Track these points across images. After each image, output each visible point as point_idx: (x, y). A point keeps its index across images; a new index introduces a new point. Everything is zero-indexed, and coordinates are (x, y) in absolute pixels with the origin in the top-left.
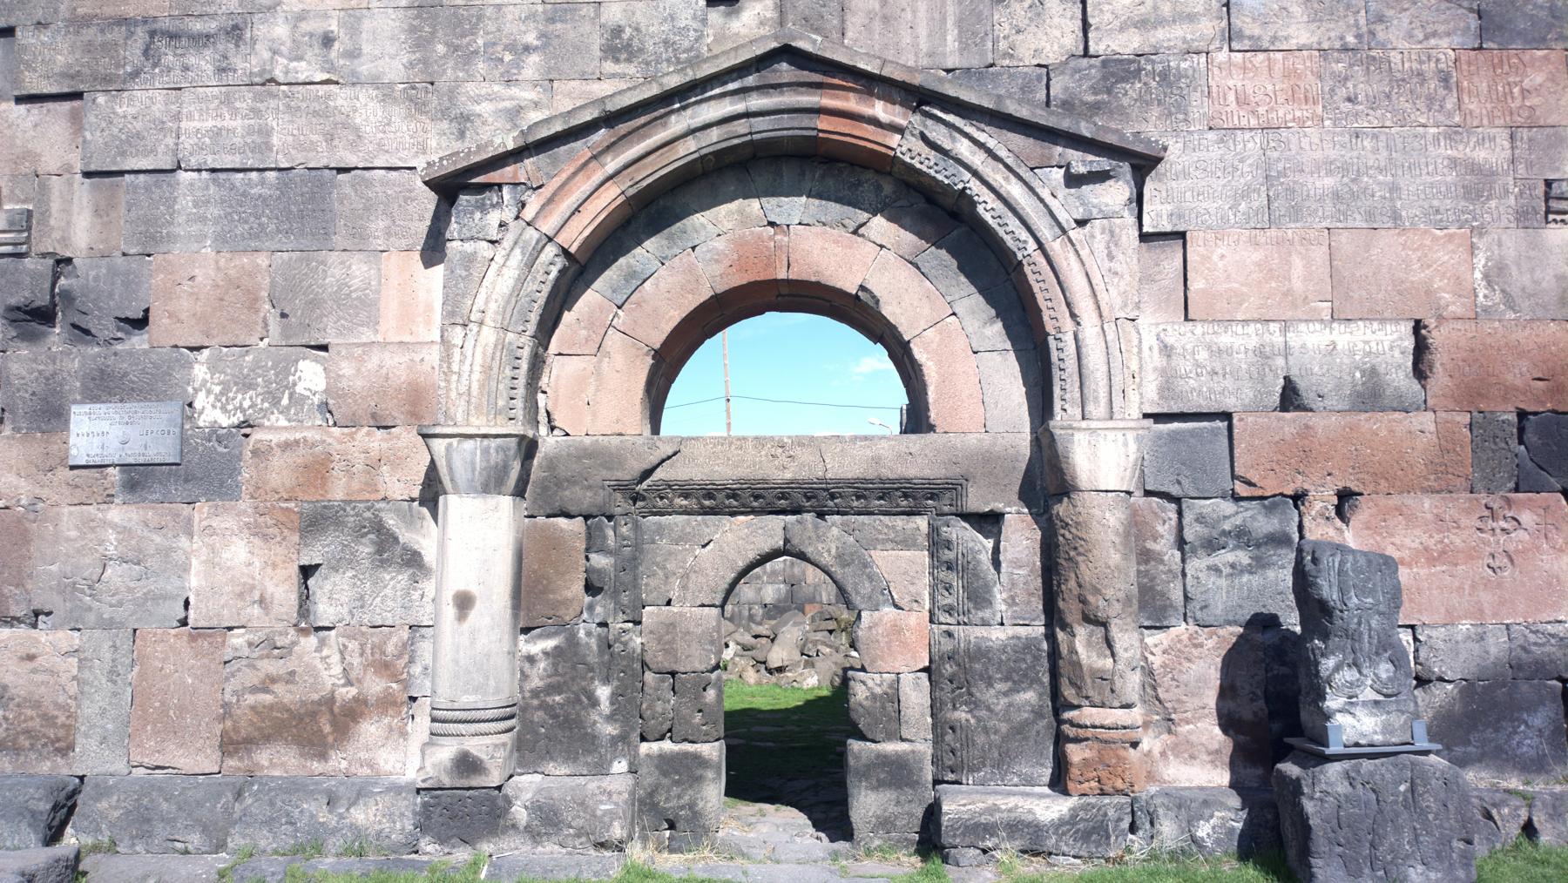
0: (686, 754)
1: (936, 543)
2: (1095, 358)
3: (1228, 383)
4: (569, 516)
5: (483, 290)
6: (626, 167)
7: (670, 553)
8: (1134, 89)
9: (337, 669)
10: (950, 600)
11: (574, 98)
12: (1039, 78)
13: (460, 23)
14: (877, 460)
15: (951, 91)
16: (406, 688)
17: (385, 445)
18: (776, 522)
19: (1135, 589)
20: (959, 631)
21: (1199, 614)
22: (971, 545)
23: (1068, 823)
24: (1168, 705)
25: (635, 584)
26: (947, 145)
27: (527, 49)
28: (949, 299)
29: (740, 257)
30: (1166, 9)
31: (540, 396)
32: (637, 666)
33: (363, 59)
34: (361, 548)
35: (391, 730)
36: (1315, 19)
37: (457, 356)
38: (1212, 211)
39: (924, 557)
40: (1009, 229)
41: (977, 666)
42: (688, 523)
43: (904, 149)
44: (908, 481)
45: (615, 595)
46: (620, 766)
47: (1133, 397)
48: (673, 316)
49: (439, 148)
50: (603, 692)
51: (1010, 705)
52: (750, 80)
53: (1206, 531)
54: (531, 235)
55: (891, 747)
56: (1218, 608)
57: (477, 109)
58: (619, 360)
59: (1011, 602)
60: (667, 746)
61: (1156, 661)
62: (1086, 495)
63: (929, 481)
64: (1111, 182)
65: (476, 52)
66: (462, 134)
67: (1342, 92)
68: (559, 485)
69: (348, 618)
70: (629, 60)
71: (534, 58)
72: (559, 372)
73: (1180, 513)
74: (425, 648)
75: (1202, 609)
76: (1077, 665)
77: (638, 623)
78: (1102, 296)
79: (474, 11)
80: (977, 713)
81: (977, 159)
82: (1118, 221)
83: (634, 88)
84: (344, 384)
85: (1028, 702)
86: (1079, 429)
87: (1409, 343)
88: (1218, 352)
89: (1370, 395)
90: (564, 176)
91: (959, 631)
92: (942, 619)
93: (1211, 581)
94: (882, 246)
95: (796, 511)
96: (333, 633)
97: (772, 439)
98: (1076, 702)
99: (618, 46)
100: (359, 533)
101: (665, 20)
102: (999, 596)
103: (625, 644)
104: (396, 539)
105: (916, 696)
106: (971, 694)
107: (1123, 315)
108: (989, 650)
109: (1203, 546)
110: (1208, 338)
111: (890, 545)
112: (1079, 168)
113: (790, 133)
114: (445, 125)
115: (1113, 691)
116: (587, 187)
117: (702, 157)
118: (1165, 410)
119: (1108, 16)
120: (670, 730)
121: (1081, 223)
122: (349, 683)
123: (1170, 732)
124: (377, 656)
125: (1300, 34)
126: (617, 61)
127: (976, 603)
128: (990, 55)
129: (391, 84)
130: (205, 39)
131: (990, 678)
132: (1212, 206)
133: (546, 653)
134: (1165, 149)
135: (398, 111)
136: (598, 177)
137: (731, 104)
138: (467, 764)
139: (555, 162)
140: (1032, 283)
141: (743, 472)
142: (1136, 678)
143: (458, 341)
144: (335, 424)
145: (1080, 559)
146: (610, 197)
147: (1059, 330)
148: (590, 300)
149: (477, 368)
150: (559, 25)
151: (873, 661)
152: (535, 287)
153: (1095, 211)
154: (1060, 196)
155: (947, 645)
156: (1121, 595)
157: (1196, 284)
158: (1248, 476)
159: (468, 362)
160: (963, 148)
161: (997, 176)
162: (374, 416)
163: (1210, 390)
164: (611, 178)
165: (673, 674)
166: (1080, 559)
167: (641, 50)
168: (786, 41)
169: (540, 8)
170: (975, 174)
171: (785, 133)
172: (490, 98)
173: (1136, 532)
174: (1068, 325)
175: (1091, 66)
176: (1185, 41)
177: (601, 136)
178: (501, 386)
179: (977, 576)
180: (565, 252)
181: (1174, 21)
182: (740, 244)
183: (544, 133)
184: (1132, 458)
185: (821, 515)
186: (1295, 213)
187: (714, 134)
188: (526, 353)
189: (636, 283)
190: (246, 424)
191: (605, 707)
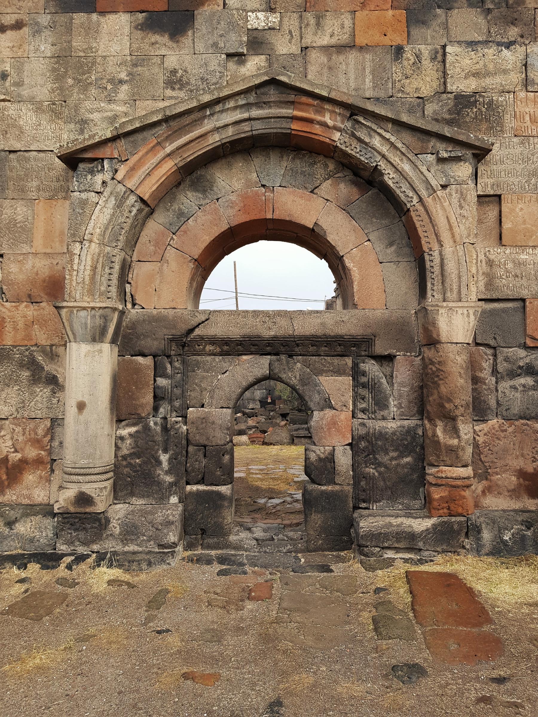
0: (213, 492)
1: (356, 373)
2: (451, 266)
3: (524, 282)
4: (144, 355)
5: (92, 221)
6: (179, 148)
7: (204, 377)
9: (9, 443)
10: (364, 405)
11: (149, 108)
12: (419, 105)
13: (82, 67)
14: (323, 324)
15: (370, 107)
16: (50, 453)
17: (35, 313)
18: (265, 360)
19: (471, 399)
20: (370, 423)
21: (504, 413)
22: (377, 374)
24: (487, 464)
25: (183, 395)
26: (367, 140)
27: (121, 82)
28: (366, 231)
29: (245, 206)
30: (491, 67)
31: (128, 287)
32: (184, 442)
33: (24, 87)
34: (23, 373)
35: (41, 477)
37: (76, 261)
38: (516, 183)
39: (348, 380)
40: (403, 189)
41: (380, 443)
42: (214, 360)
43: (342, 141)
44: (342, 337)
45: (171, 401)
46: (174, 500)
47: (473, 289)
48: (206, 239)
49: (67, 137)
50: (164, 458)
51: (398, 465)
52: (252, 98)
53: (510, 366)
54: (120, 188)
55: (330, 488)
56: (515, 410)
57: (91, 116)
58: (173, 265)
59: (399, 406)
60: (201, 487)
61: (481, 440)
62: (445, 345)
63: (353, 337)
64: (462, 163)
65: (91, 84)
66: (82, 132)
68: (138, 338)
69: (16, 413)
70: (180, 89)
71: (125, 88)
72: (140, 272)
73: (495, 355)
74: (58, 430)
75: (506, 410)
76: (438, 442)
77: (185, 417)
78: (456, 230)
79: (90, 59)
80: (379, 469)
81: (385, 149)
82: (466, 186)
83: (183, 102)
84: (12, 277)
85: (408, 463)
86: (442, 307)
88: (519, 264)
90: (141, 154)
91: (370, 423)
92: (359, 416)
93: (511, 394)
94: (327, 200)
95: (276, 354)
96: (7, 422)
97: (263, 312)
98: (436, 464)
99: (174, 81)
100: (21, 365)
101: (202, 66)
102: (392, 402)
103: (178, 430)
104: (43, 368)
105: (344, 459)
106: (376, 459)
107: (467, 241)
108: (387, 433)
109: (507, 375)
110: (513, 256)
111: (330, 374)
112: (445, 155)
113: (275, 131)
114: (72, 126)
115: (457, 457)
116: (154, 160)
117: (223, 145)
118: (489, 297)
119: (458, 70)
120: (203, 479)
121: (444, 187)
122: (16, 451)
123: (487, 479)
124: (33, 436)
126: (173, 89)
127: (379, 407)
128: (390, 90)
129: (41, 102)
131: (387, 449)
132: (516, 181)
133: (130, 435)
134: (493, 144)
135: (44, 119)
136: (161, 154)
137: (240, 113)
139: (135, 146)
140: (415, 221)
141: (246, 331)
142: (470, 450)
143: (77, 251)
144: (7, 301)
145: (441, 382)
146: (169, 166)
147: (431, 250)
149: (88, 268)
150: (140, 68)
151: (320, 439)
152: (123, 220)
153: (452, 180)
154: (432, 171)
155: (362, 431)
156: (464, 403)
157: (507, 225)
158: (534, 335)
159: (83, 264)
160: (376, 142)
161: (395, 159)
162: (29, 296)
163: (513, 285)
164: (169, 155)
165: (205, 446)
166: (441, 382)
167: (188, 83)
168: (273, 76)
169: (129, 58)
170: (383, 156)
171: (272, 131)
173: (473, 365)
174: (436, 247)
175: (449, 99)
176: (501, 85)
178: (103, 278)
179: (381, 392)
180: (142, 200)
181: (496, 73)
182: (244, 197)
183: (130, 128)
184: (471, 325)
185: (291, 356)
187: (230, 131)
188: (118, 260)
189: (183, 219)
191: (165, 465)
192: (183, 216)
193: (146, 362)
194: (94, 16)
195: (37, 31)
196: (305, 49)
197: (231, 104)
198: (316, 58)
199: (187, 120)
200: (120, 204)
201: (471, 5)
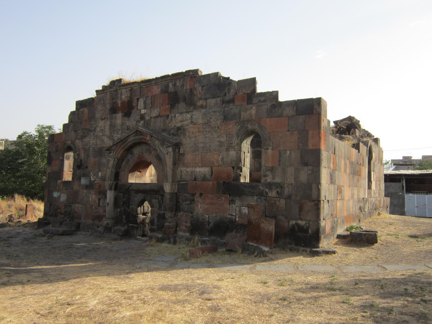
8: (180, 131)
23: (161, 238)
27: (120, 130)
36: (202, 119)
46: (126, 227)
50: (124, 217)
67: (205, 130)
71: (120, 131)
77: (129, 208)
87: (210, 171)
88: (187, 172)
89: (204, 179)
99: (128, 129)
116: (120, 150)
125: (200, 121)
130: (92, 131)
138: (108, 224)
148: (124, 163)
172: (116, 137)
177: (121, 143)
186: (198, 150)
190: (95, 180)
192: (129, 160)
193: (121, 194)
194: (116, 115)
195: (107, 120)
196: (151, 118)
197: (132, 136)
198: (153, 119)
199: (125, 140)
200: (114, 160)
201: (183, 102)
